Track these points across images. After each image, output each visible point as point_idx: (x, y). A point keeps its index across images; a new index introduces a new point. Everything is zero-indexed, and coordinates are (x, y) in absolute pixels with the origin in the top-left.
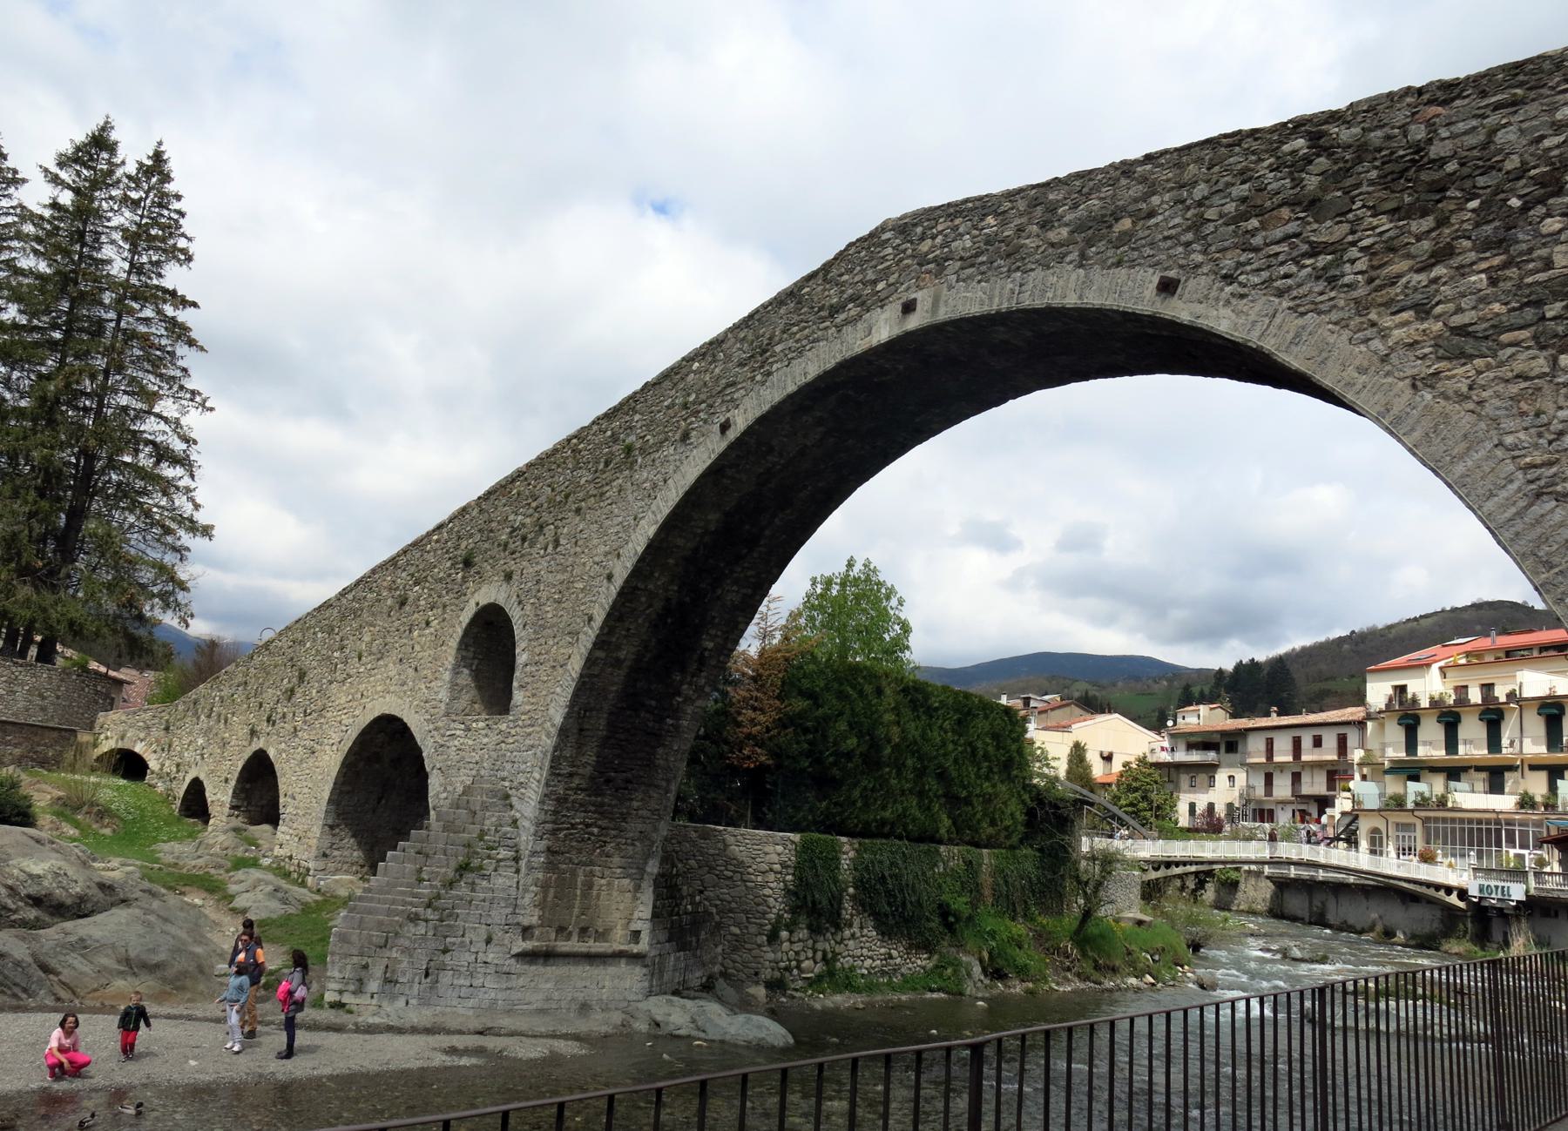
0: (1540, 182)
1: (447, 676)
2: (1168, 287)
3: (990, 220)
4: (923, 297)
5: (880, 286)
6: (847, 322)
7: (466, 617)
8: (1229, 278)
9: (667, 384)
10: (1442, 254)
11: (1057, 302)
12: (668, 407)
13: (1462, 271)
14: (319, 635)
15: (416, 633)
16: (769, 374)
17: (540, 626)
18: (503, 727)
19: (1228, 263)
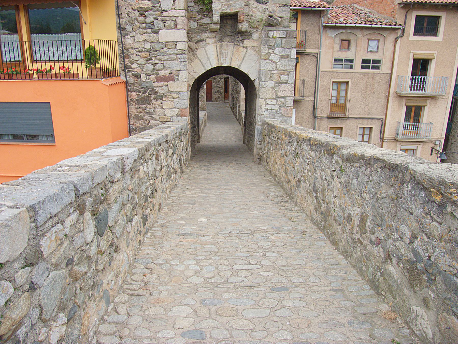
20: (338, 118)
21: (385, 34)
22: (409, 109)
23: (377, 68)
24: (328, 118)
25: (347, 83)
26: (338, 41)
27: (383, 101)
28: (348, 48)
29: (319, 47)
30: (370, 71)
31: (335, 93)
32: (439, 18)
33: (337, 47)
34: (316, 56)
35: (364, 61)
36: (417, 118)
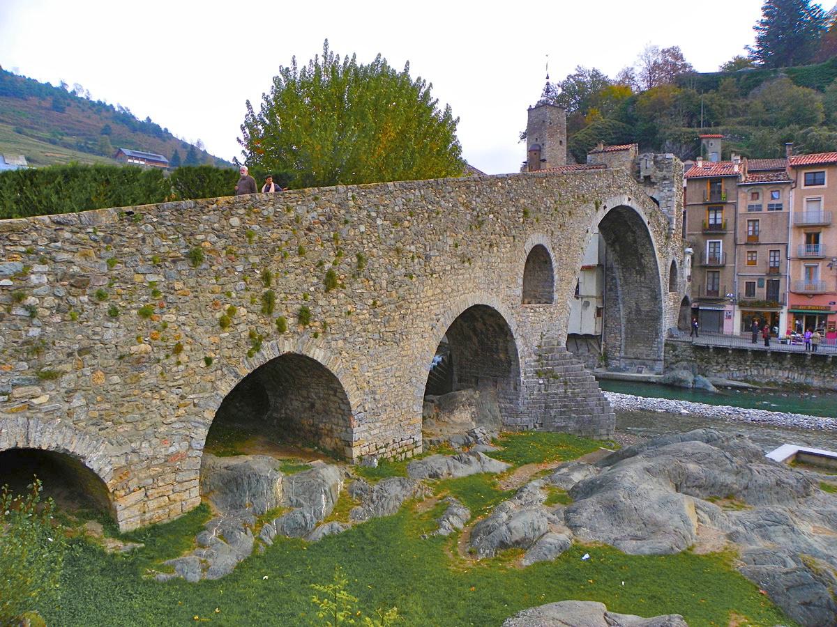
1: (520, 282)
2: (649, 223)
7: (528, 247)
14: (379, 222)
20: (752, 244)
21: (783, 187)
22: (808, 236)
23: (781, 209)
24: (746, 244)
25: (758, 220)
26: (750, 194)
27: (785, 232)
28: (758, 198)
29: (737, 198)
30: (775, 211)
31: (751, 228)
32: (824, 172)
34: (735, 205)
35: (769, 205)
36: (817, 241)
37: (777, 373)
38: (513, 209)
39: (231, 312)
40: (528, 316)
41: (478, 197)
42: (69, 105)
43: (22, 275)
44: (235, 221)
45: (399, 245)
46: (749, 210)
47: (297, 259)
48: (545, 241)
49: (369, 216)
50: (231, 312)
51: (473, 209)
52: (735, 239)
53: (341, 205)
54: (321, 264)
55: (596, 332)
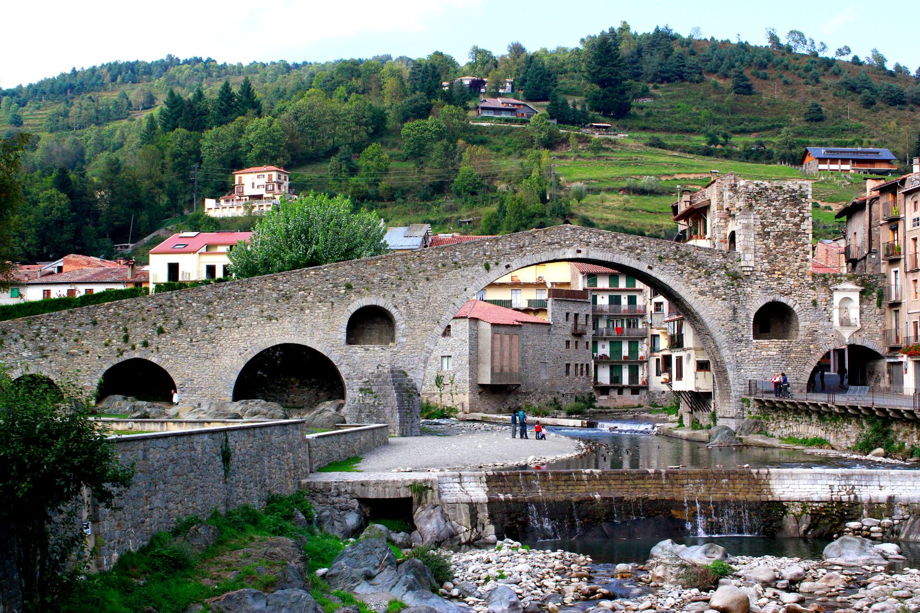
0: (714, 270)
2: (650, 268)
3: (601, 237)
4: (584, 250)
5: (567, 242)
6: (555, 248)
8: (662, 270)
9: (472, 245)
10: (700, 277)
11: (623, 263)
12: (476, 254)
13: (702, 281)
14: (194, 304)
15: (307, 311)
16: (525, 255)
17: (411, 316)
18: (396, 349)
19: (662, 268)
26: (913, 204)
33: (913, 208)
37: (808, 429)
38: (331, 285)
39: (110, 341)
40: (356, 353)
41: (286, 283)
42: (765, 78)
43: (39, 329)
44: (112, 310)
45: (211, 314)
46: (914, 226)
47: (141, 322)
48: (381, 303)
49: (187, 303)
50: (110, 341)
51: (281, 291)
52: (905, 265)
53: (168, 300)
54: (155, 324)
55: (696, 388)
